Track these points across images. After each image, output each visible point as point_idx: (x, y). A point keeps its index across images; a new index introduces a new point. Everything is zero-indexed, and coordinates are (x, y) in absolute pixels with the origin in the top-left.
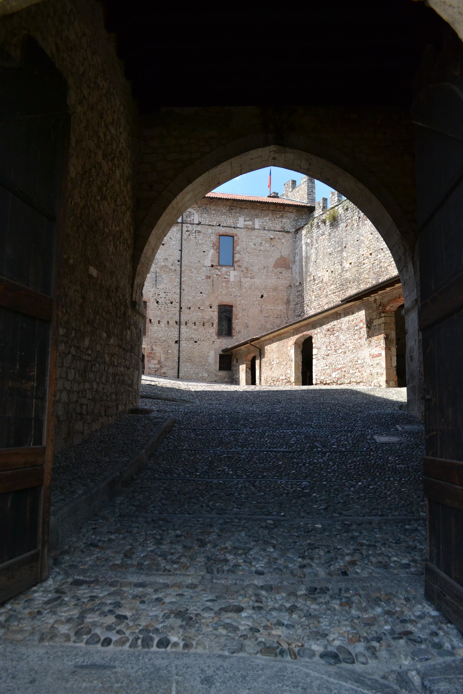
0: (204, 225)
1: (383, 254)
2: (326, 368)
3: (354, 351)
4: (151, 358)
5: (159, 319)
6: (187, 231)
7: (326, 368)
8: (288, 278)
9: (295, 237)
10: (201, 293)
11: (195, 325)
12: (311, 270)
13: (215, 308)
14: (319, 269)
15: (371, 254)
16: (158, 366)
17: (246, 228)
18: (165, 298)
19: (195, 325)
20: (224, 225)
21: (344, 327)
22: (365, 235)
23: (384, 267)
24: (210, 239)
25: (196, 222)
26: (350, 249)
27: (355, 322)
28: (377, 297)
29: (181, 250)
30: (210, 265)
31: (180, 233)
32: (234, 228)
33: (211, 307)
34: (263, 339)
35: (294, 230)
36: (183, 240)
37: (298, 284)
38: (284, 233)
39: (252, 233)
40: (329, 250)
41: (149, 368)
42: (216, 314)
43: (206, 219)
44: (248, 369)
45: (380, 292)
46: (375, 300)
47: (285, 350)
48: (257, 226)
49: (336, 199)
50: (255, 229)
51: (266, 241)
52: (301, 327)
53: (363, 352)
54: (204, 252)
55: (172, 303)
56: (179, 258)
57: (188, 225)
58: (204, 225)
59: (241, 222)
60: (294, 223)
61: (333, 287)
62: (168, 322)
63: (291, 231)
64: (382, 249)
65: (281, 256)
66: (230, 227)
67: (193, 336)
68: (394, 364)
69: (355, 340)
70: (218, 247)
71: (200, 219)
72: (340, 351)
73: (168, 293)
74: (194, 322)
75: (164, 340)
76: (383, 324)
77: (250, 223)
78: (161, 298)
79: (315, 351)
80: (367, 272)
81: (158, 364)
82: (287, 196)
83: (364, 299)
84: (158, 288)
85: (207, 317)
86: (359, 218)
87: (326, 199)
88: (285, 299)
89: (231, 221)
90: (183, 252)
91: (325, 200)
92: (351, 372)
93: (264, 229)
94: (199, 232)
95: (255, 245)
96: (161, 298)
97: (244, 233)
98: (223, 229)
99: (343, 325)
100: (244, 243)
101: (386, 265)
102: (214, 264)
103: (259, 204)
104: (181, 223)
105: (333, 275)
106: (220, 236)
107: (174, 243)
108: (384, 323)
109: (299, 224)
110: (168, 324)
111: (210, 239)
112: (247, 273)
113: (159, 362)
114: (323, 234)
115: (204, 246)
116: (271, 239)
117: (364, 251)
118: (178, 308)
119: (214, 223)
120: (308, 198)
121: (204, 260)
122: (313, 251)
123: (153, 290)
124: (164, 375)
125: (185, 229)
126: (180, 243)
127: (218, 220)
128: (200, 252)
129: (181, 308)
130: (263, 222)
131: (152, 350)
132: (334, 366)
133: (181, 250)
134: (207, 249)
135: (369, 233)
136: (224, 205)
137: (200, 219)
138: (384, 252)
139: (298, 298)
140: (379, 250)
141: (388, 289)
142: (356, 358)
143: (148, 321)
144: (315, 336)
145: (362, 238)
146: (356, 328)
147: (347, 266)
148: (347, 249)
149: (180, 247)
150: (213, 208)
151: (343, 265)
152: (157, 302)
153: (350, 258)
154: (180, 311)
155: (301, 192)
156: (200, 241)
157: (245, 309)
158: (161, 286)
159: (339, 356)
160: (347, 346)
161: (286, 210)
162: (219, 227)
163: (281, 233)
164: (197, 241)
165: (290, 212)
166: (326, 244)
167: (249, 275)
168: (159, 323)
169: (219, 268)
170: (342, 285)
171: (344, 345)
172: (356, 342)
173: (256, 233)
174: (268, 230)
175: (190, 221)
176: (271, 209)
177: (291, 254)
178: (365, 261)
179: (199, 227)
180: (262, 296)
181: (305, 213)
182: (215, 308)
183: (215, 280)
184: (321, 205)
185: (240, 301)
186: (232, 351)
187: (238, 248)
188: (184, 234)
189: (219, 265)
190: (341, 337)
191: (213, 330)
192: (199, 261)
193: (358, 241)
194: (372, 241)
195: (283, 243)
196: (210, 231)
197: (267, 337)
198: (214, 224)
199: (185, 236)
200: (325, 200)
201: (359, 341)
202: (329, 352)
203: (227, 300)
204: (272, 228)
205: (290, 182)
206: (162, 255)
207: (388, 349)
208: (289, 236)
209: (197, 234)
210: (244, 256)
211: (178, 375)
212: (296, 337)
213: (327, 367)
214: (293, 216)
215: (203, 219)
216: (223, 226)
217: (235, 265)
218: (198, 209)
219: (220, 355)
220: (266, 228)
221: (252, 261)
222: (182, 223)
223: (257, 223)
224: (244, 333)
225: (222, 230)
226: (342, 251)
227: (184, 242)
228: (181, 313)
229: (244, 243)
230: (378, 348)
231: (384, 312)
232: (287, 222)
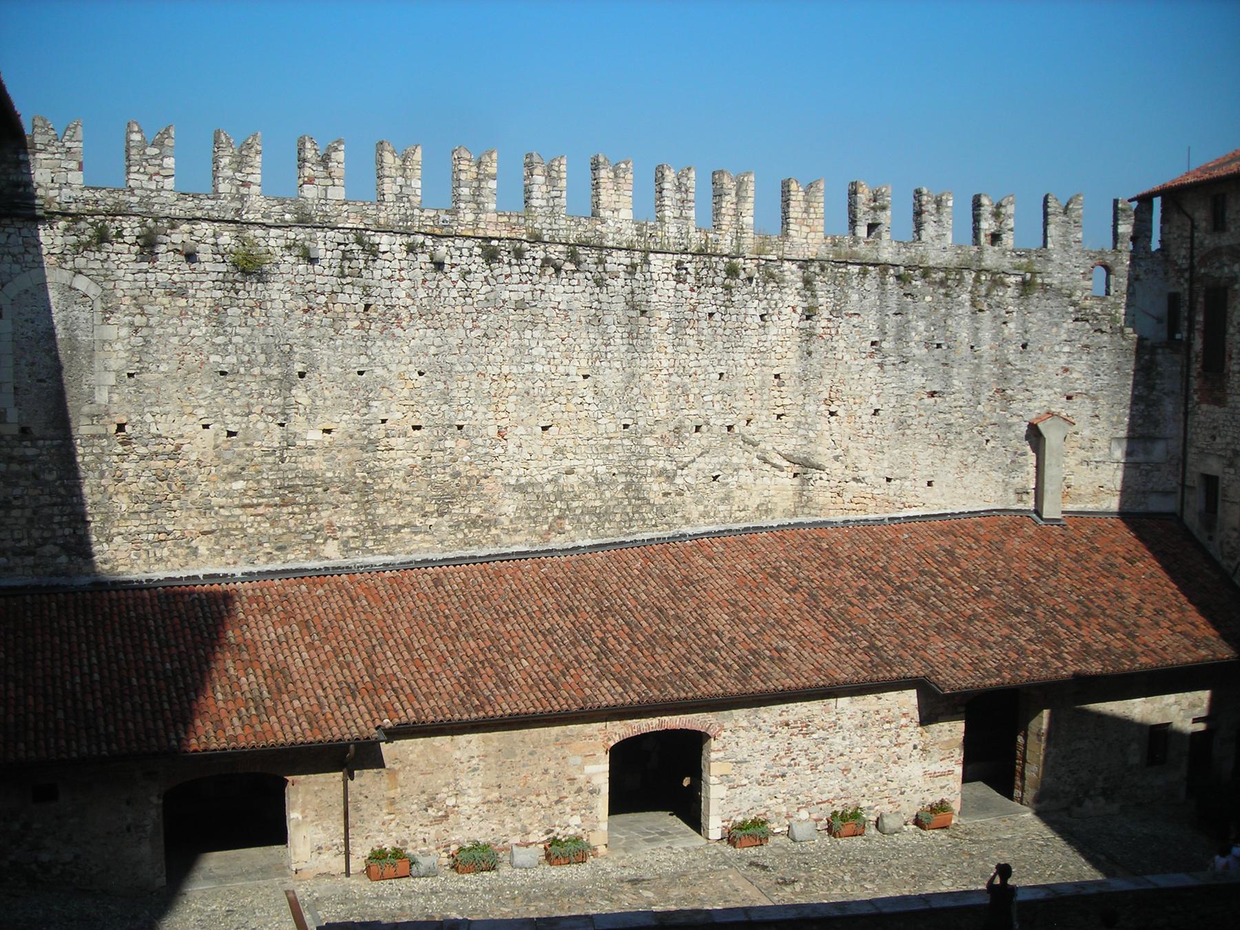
1: (463, 443)
12: (102, 397)
61: (239, 485)
64: (460, 427)
80: (402, 473)
140: (450, 426)
178: (393, 441)
193: (361, 373)
194: (424, 394)
212: (621, 730)
226: (286, 383)
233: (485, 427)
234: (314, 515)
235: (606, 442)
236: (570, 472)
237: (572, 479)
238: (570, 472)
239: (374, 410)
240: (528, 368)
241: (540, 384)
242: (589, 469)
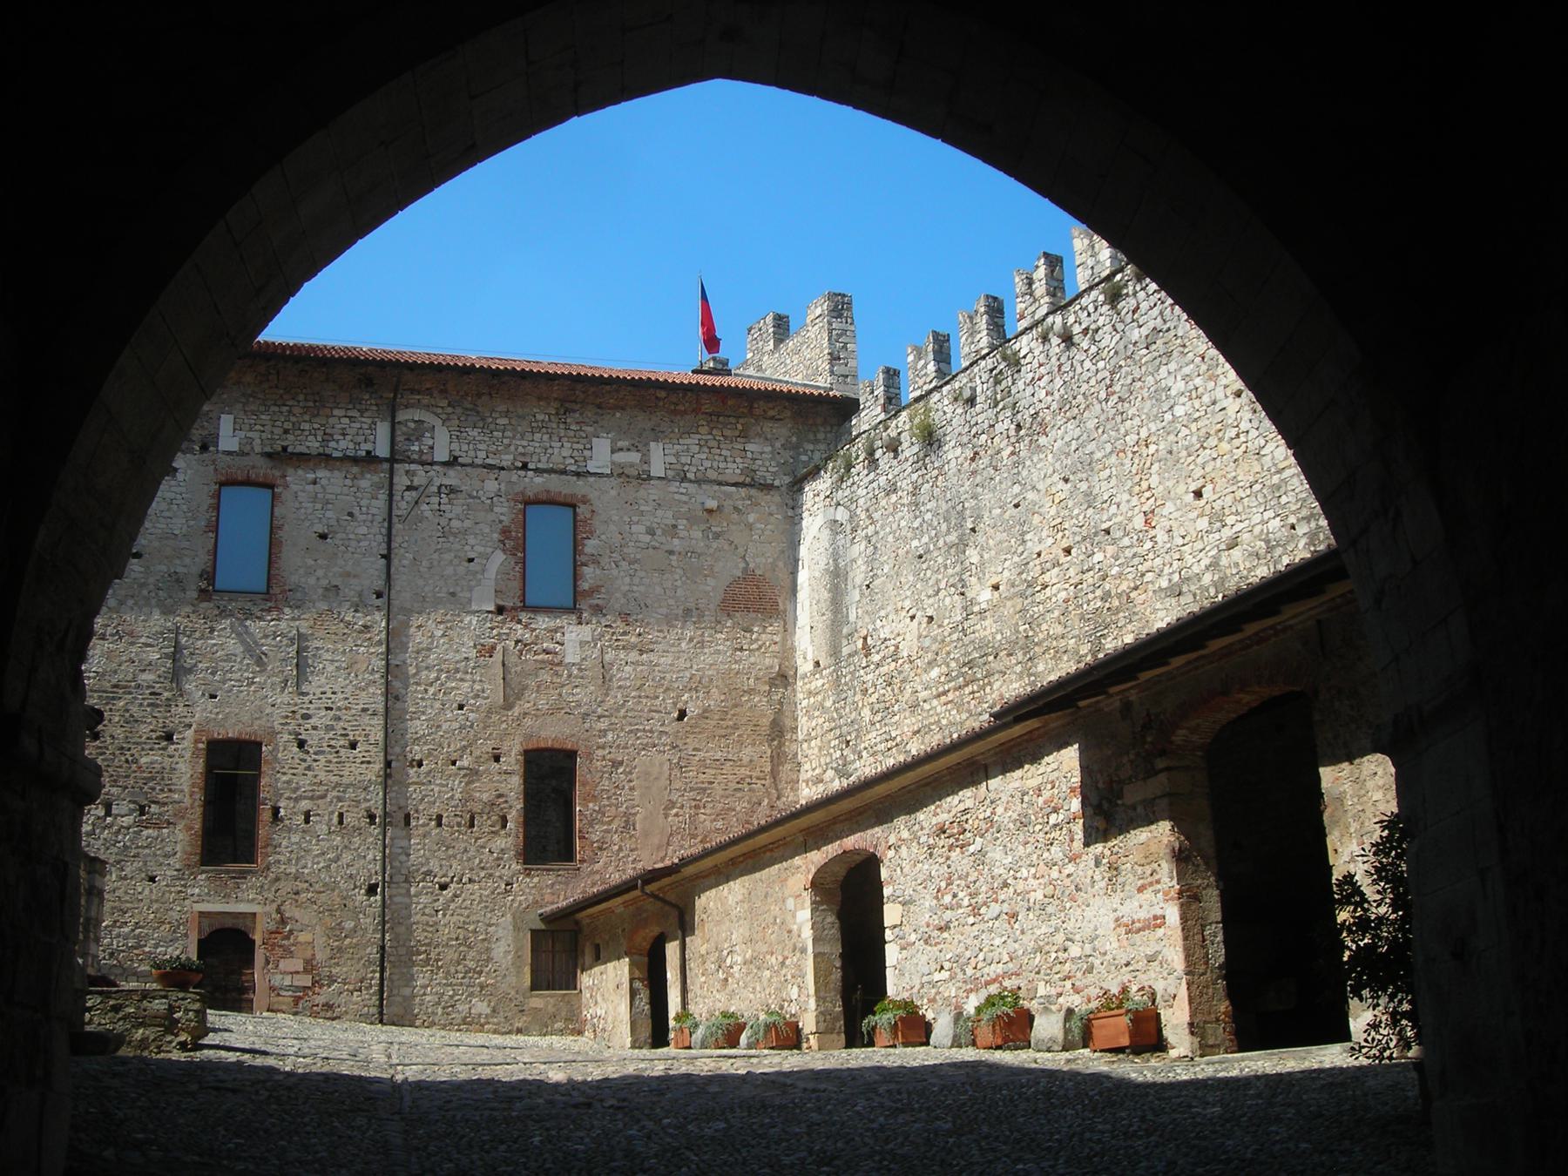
0: (472, 465)
1: (1111, 550)
2: (937, 976)
3: (1050, 909)
4: (279, 951)
5: (305, 805)
6: (409, 488)
7: (937, 976)
8: (773, 648)
9: (790, 502)
10: (461, 707)
11: (439, 824)
12: (852, 617)
13: (512, 760)
14: (882, 613)
15: (1068, 551)
16: (306, 981)
17: (621, 474)
18: (329, 728)
19: (439, 824)
20: (540, 466)
21: (1004, 816)
22: (1041, 486)
23: (1119, 596)
24: (491, 517)
25: (441, 455)
26: (990, 536)
27: (1046, 794)
28: (1133, 696)
29: (387, 557)
30: (492, 608)
31: (383, 496)
32: (578, 474)
33: (497, 759)
34: (690, 870)
35: (787, 479)
36: (395, 520)
37: (809, 666)
38: (753, 492)
39: (642, 493)
40: (915, 543)
41: (273, 989)
42: (516, 781)
43: (476, 445)
44: (638, 984)
45: (1145, 676)
46: (1127, 707)
47: (775, 909)
48: (657, 469)
49: (931, 367)
50: (650, 478)
51: (692, 520)
52: (835, 821)
53: (1089, 913)
54: (471, 560)
55: (353, 746)
56: (379, 584)
57: (413, 467)
58: (472, 465)
59: (601, 455)
60: (787, 455)
61: (935, 673)
62: (341, 815)
63: (777, 483)
64: (1107, 532)
65: (745, 570)
66: (564, 472)
67: (434, 865)
68: (1218, 954)
69: (1051, 864)
70: (516, 541)
71: (455, 446)
72: (995, 908)
73: (339, 709)
74: (435, 810)
75: (325, 885)
76: (1165, 801)
77: (634, 457)
78: (315, 728)
79: (891, 913)
80: (1056, 613)
81: (306, 971)
82: (759, 368)
83: (1082, 704)
84: (303, 694)
85: (485, 797)
86: (1019, 427)
87: (896, 373)
88: (766, 722)
89: (566, 453)
90: (395, 562)
91: (892, 375)
92: (1042, 991)
93: (684, 479)
94: (452, 490)
95: (651, 532)
96: (315, 728)
97: (613, 493)
98: (539, 480)
99: (1000, 810)
100: (612, 527)
101: (1124, 586)
102: (508, 604)
103: (663, 394)
104: (386, 460)
105: (936, 631)
106: (528, 503)
107: (363, 530)
108: (1169, 795)
109: (804, 458)
110: (341, 822)
111: (491, 517)
112: (625, 633)
113: (310, 966)
114: (892, 489)
115: (472, 541)
116: (710, 511)
117: (1043, 542)
118: (378, 766)
119: (507, 459)
120: (832, 373)
121: (471, 590)
122: (859, 548)
123: (285, 698)
124: (329, 1014)
125: (401, 481)
126: (384, 531)
127: (521, 450)
128: (456, 561)
129: (388, 764)
130: (677, 455)
131: (283, 921)
132: (970, 971)
133: (387, 557)
134: (479, 549)
135: (1056, 477)
136: (540, 398)
137: (455, 446)
138: (1114, 542)
139: (811, 718)
140: (1096, 534)
141: (1177, 661)
142: (1060, 938)
143: (265, 815)
144: (891, 853)
145: (1031, 496)
146: (1053, 819)
147: (985, 596)
148: (980, 538)
149: (384, 546)
150: (502, 408)
151: (970, 595)
152: (301, 744)
153: (993, 569)
154: (387, 776)
155: (807, 353)
156: (455, 523)
157: (621, 763)
158: (316, 684)
159: (991, 930)
160: (1020, 888)
161: (757, 412)
162: (522, 473)
163: (743, 491)
164: (443, 522)
165: (772, 418)
166: (903, 523)
167: (634, 639)
168: (307, 821)
169: (524, 617)
170: (970, 664)
171: (1006, 885)
172: (1055, 874)
173: (653, 491)
174: (698, 482)
175: (421, 451)
176: (707, 408)
177: (781, 564)
178: (1047, 577)
179: (451, 472)
180: (682, 715)
181: (824, 423)
182: (512, 760)
183: (512, 659)
184: (880, 391)
185: (603, 733)
186: (580, 916)
187: (591, 546)
188: (397, 498)
189: (525, 608)
190: (996, 854)
191: (508, 841)
192: (453, 594)
193: (1017, 506)
194: (1070, 503)
195: (750, 527)
196: (491, 486)
197: (708, 863)
198: (504, 464)
199: (401, 507)
200: (892, 375)
201: (1070, 868)
202: (948, 915)
203: (552, 733)
204: (712, 475)
205: (769, 319)
206: (320, 573)
207: (1189, 898)
208: (770, 502)
209: (445, 499)
210: (615, 572)
211: (381, 1013)
212: (817, 858)
213: (945, 975)
214: (782, 431)
215: (465, 447)
216: (536, 470)
217: (583, 605)
218: (450, 410)
219: (533, 931)
220: (690, 476)
221: (642, 589)
222: (392, 460)
223: (659, 458)
224: (620, 849)
225: (535, 483)
226: (962, 545)
227: (397, 527)
228: (390, 782)
229: (612, 527)
230: (1148, 894)
231: (1163, 753)
232: (764, 452)
233: (1130, 519)
234: (988, 689)
235: (1276, 479)
236: (1233, 544)
237: (1236, 553)
238: (1233, 544)
239: (1029, 544)
240: (1168, 417)
241: (1185, 431)
242: (1257, 530)
